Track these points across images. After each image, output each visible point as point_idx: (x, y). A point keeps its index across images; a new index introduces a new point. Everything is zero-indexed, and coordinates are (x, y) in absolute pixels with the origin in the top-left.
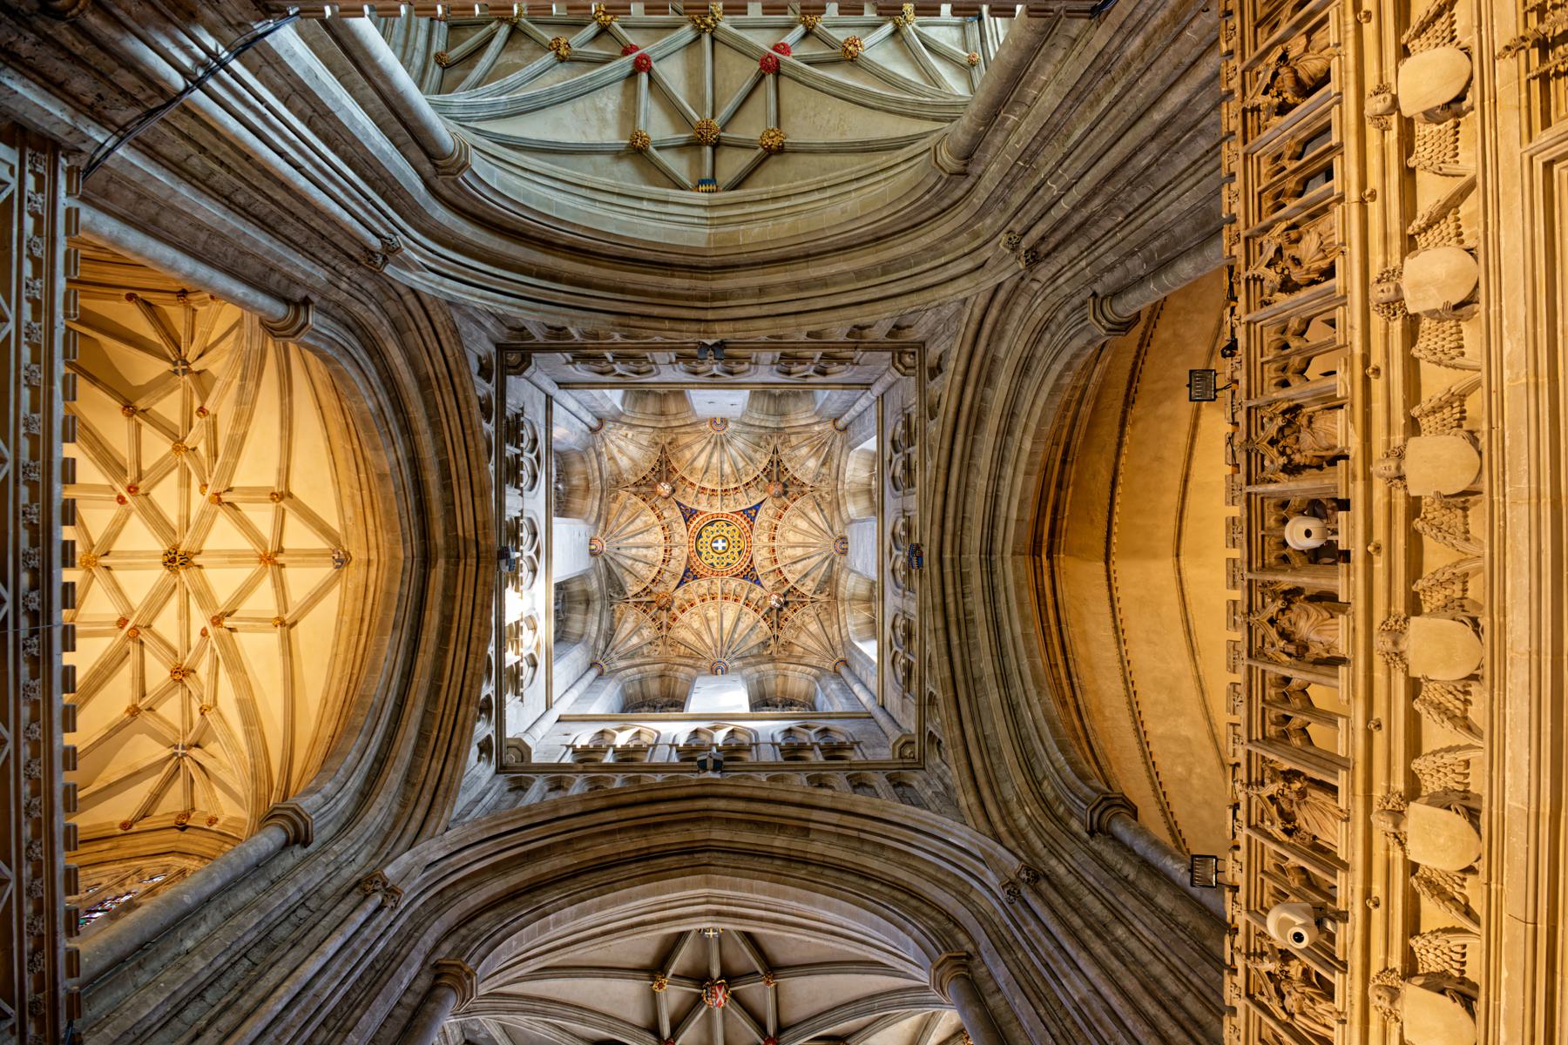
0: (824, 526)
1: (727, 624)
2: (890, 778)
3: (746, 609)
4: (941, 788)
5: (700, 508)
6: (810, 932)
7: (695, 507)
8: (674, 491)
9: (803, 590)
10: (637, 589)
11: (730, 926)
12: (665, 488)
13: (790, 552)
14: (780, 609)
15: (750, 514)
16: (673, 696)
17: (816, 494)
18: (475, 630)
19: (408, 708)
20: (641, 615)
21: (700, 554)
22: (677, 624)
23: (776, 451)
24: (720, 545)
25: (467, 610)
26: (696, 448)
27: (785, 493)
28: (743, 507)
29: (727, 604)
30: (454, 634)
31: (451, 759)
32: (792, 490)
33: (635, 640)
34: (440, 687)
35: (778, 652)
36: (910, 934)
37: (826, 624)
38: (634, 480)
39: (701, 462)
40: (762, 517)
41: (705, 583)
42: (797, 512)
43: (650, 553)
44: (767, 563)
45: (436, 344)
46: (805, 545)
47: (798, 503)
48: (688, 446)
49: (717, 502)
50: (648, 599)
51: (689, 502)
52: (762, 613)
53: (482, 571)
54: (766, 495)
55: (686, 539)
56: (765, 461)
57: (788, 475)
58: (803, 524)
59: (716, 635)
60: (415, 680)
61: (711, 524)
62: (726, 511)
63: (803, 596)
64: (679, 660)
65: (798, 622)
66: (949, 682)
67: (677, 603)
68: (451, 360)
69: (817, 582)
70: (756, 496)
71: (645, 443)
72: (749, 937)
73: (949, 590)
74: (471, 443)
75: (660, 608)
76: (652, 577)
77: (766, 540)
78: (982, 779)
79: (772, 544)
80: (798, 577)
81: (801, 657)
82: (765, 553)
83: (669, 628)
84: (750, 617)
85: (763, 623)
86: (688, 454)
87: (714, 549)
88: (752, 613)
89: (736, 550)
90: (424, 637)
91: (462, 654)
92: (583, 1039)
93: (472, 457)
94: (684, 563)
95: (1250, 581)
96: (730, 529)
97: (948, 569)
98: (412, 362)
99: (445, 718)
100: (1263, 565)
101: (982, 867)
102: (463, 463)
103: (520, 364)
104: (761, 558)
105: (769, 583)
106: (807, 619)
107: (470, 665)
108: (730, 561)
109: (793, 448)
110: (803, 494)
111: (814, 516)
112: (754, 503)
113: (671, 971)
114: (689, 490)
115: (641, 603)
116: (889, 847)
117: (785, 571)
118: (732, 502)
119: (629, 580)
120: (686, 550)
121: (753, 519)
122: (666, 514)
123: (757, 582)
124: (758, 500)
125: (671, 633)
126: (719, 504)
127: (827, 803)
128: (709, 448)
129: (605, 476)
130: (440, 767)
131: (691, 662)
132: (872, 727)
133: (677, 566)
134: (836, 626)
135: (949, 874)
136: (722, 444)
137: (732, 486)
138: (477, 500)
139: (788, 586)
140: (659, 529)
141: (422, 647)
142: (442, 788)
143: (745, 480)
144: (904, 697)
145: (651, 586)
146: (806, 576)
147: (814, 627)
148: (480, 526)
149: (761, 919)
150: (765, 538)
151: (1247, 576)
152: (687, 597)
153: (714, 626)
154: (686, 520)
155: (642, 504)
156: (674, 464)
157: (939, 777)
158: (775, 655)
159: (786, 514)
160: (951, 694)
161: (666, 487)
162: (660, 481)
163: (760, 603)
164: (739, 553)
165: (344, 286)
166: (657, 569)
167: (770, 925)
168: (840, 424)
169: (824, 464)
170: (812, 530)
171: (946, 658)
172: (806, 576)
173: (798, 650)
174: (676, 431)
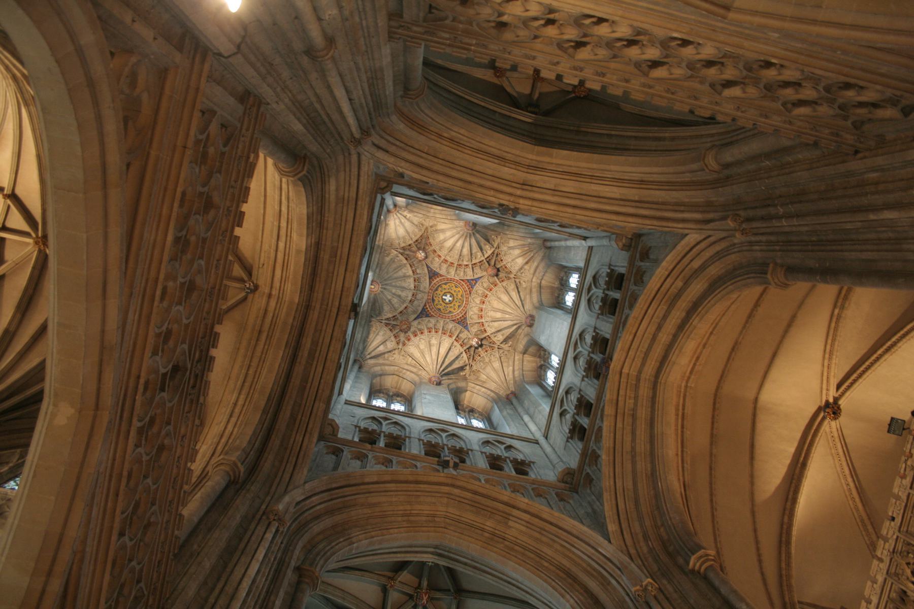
0: (519, 303)
1: (443, 351)
2: (557, 494)
3: (456, 343)
4: (590, 510)
5: (441, 272)
6: (494, 579)
7: (438, 271)
8: (426, 257)
9: (495, 339)
10: (390, 315)
11: (442, 562)
12: (421, 255)
13: (492, 314)
14: (476, 348)
15: (472, 283)
16: (399, 389)
17: (517, 281)
18: (330, 355)
19: (287, 398)
20: (388, 332)
21: (433, 300)
23: (498, 247)
25: (327, 340)
26: (448, 234)
27: (497, 275)
28: (468, 278)
29: (444, 337)
30: (317, 354)
31: (307, 435)
32: (501, 275)
33: (381, 348)
34: (305, 387)
35: (470, 375)
36: (568, 601)
37: (504, 364)
38: (403, 245)
39: (449, 244)
40: (479, 288)
41: (433, 321)
42: (503, 289)
43: (403, 294)
44: (475, 317)
45: (356, 182)
46: (503, 312)
47: (504, 284)
48: (443, 231)
49: (452, 271)
50: (395, 323)
51: (435, 266)
52: (465, 348)
53: (339, 317)
54: (485, 273)
55: (427, 290)
56: (490, 252)
57: (502, 264)
58: (505, 298)
59: (434, 357)
60: (293, 380)
61: (445, 284)
62: (457, 278)
63: (494, 343)
64: (406, 367)
65: (487, 360)
66: (612, 450)
67: (412, 329)
68: (361, 191)
70: (479, 273)
72: (451, 572)
73: (622, 392)
74: (354, 239)
75: (401, 330)
76: (400, 310)
77: (478, 302)
78: (623, 517)
79: (481, 306)
80: (493, 330)
81: (484, 382)
82: (475, 310)
83: (404, 344)
84: (457, 349)
85: (464, 354)
86: (441, 237)
87: (444, 300)
88: (459, 346)
89: (457, 304)
90: (300, 354)
91: (320, 369)
92: (334, 604)
93: (353, 248)
94: (422, 305)
95: (898, 537)
96: (457, 290)
97: (623, 380)
98: (337, 190)
99: (306, 408)
100: (907, 531)
101: (619, 573)
102: (346, 250)
103: (385, 188)
104: (473, 313)
105: (474, 329)
107: (324, 376)
108: (452, 310)
109: (510, 248)
110: (509, 278)
111: (514, 295)
112: (476, 277)
113: (399, 579)
114: (437, 259)
115: (389, 324)
116: (557, 542)
117: (486, 325)
118: (462, 274)
119: (386, 308)
120: (426, 297)
122: (418, 271)
123: (466, 327)
124: (479, 275)
125: (406, 348)
126: (453, 273)
127: (523, 506)
128: (457, 236)
129: (386, 239)
130: (301, 439)
131: (414, 370)
132: (538, 451)
133: (419, 305)
134: (511, 368)
135: (595, 569)
137: (465, 263)
138: (348, 274)
139: (486, 334)
140: (412, 279)
141: (298, 360)
142: (302, 453)
143: (474, 262)
144: (567, 441)
145: (398, 316)
146: (499, 331)
147: (497, 365)
148: (345, 289)
149: (466, 564)
150: (478, 301)
151: (897, 534)
152: (419, 327)
153: (434, 350)
154: (430, 278)
155: (405, 261)
156: (431, 240)
157: (589, 503)
158: (467, 376)
159: (495, 289)
160: (612, 458)
161: (423, 254)
162: (419, 249)
163: (465, 341)
164: (459, 306)
165: (328, 151)
166: (405, 305)
167: (470, 568)
168: (548, 244)
169: (527, 263)
170: (510, 303)
171: (612, 435)
172: (499, 331)
173: (483, 377)
174: (439, 220)
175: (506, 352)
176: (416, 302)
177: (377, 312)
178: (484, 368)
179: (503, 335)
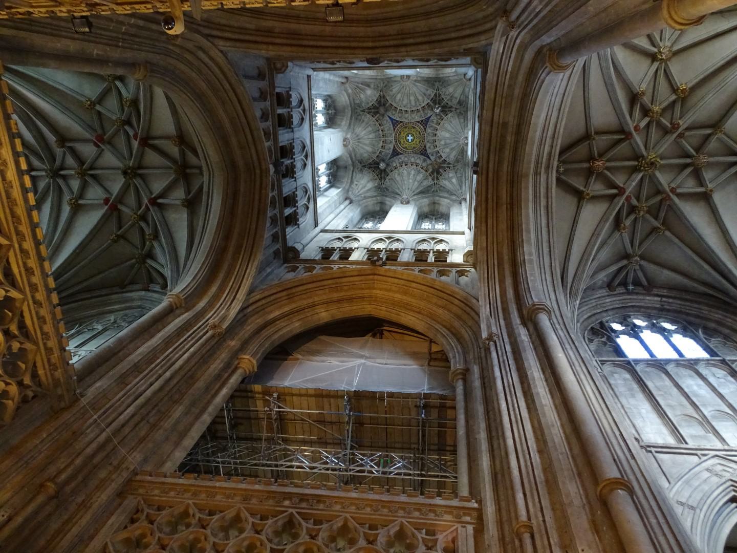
7: (391, 150)
9: (433, 95)
22: (447, 160)
24: (410, 138)
33: (454, 180)
41: (428, 145)
65: (448, 97)
69: (428, 88)
71: (361, 175)
83: (449, 164)
94: (419, 156)
106: (447, 93)
112: (389, 120)
115: (437, 177)
121: (397, 121)
122: (395, 165)
124: (388, 119)
136: (359, 139)
137: (381, 132)
146: (425, 94)
161: (381, 165)
162: (378, 168)
175: (441, 83)
176: (418, 162)
177: (429, 188)
178: (456, 98)
179: (427, 90)
